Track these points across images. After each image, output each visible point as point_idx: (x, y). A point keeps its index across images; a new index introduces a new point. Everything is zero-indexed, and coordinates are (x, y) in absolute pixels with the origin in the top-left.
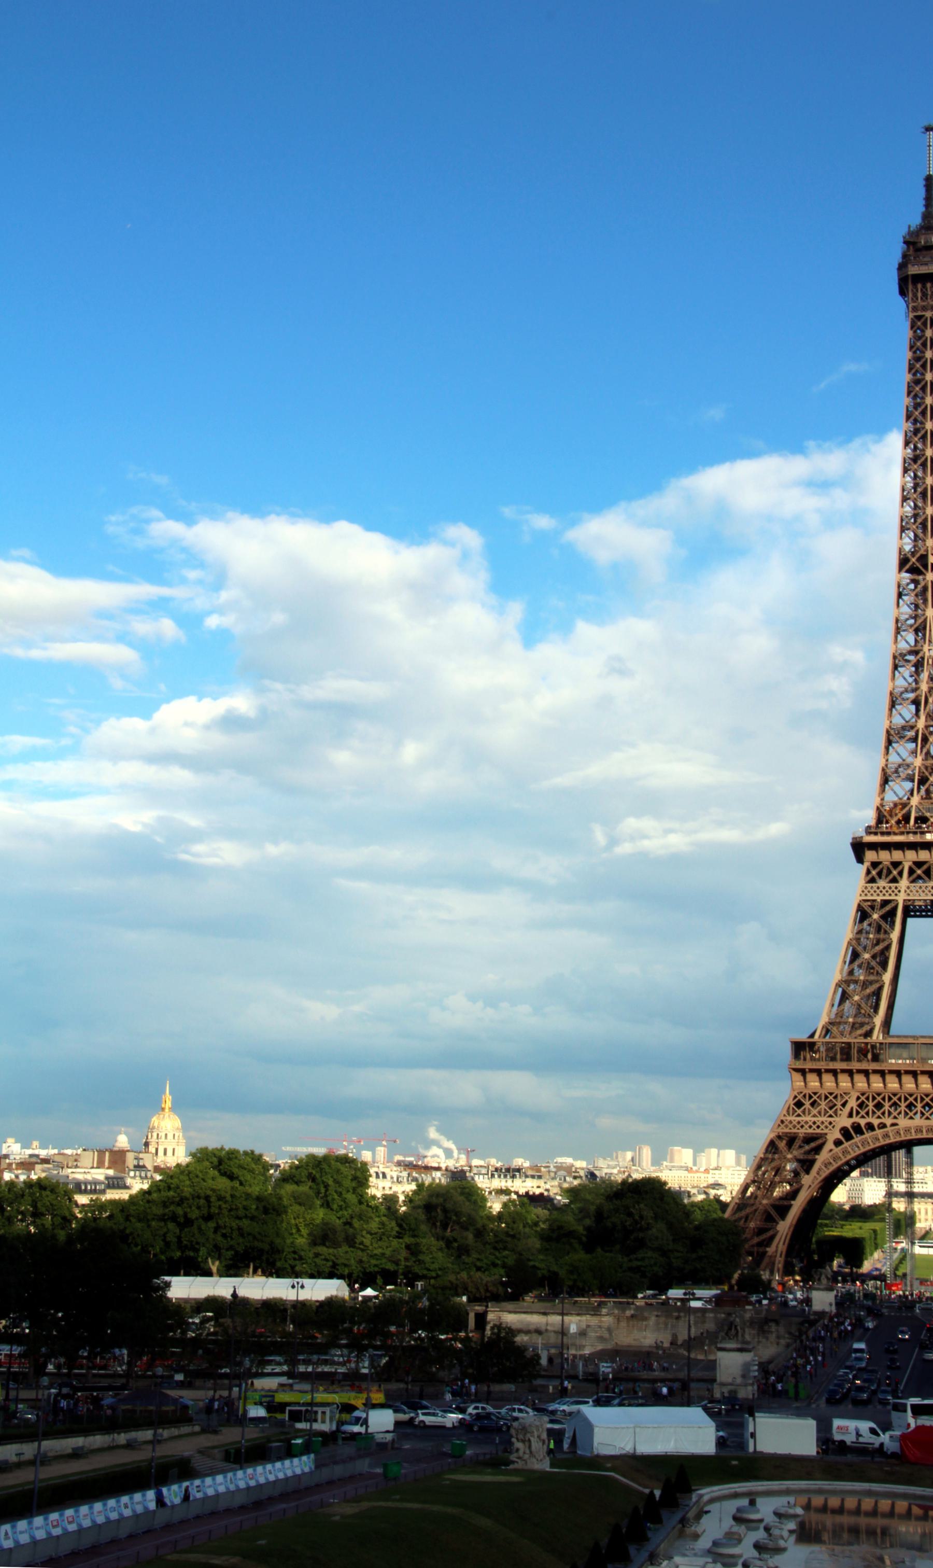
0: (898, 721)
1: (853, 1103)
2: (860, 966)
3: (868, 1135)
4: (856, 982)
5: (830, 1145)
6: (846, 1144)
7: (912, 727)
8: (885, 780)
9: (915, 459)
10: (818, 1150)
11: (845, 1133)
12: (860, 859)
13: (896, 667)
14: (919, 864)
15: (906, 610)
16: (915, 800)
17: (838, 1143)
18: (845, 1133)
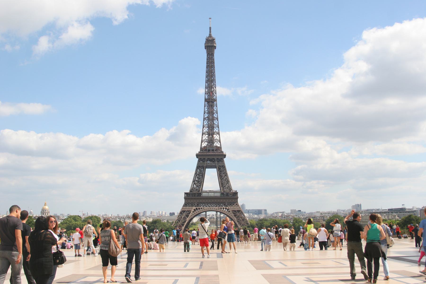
0: (204, 131)
1: (196, 204)
2: (197, 178)
3: (199, 210)
4: (196, 181)
5: (192, 212)
6: (195, 212)
7: (207, 132)
8: (202, 142)
9: (208, 80)
10: (190, 213)
11: (195, 210)
12: (197, 157)
13: (204, 120)
14: (208, 159)
15: (206, 109)
16: (208, 146)
17: (193, 212)
18: (195, 210)
